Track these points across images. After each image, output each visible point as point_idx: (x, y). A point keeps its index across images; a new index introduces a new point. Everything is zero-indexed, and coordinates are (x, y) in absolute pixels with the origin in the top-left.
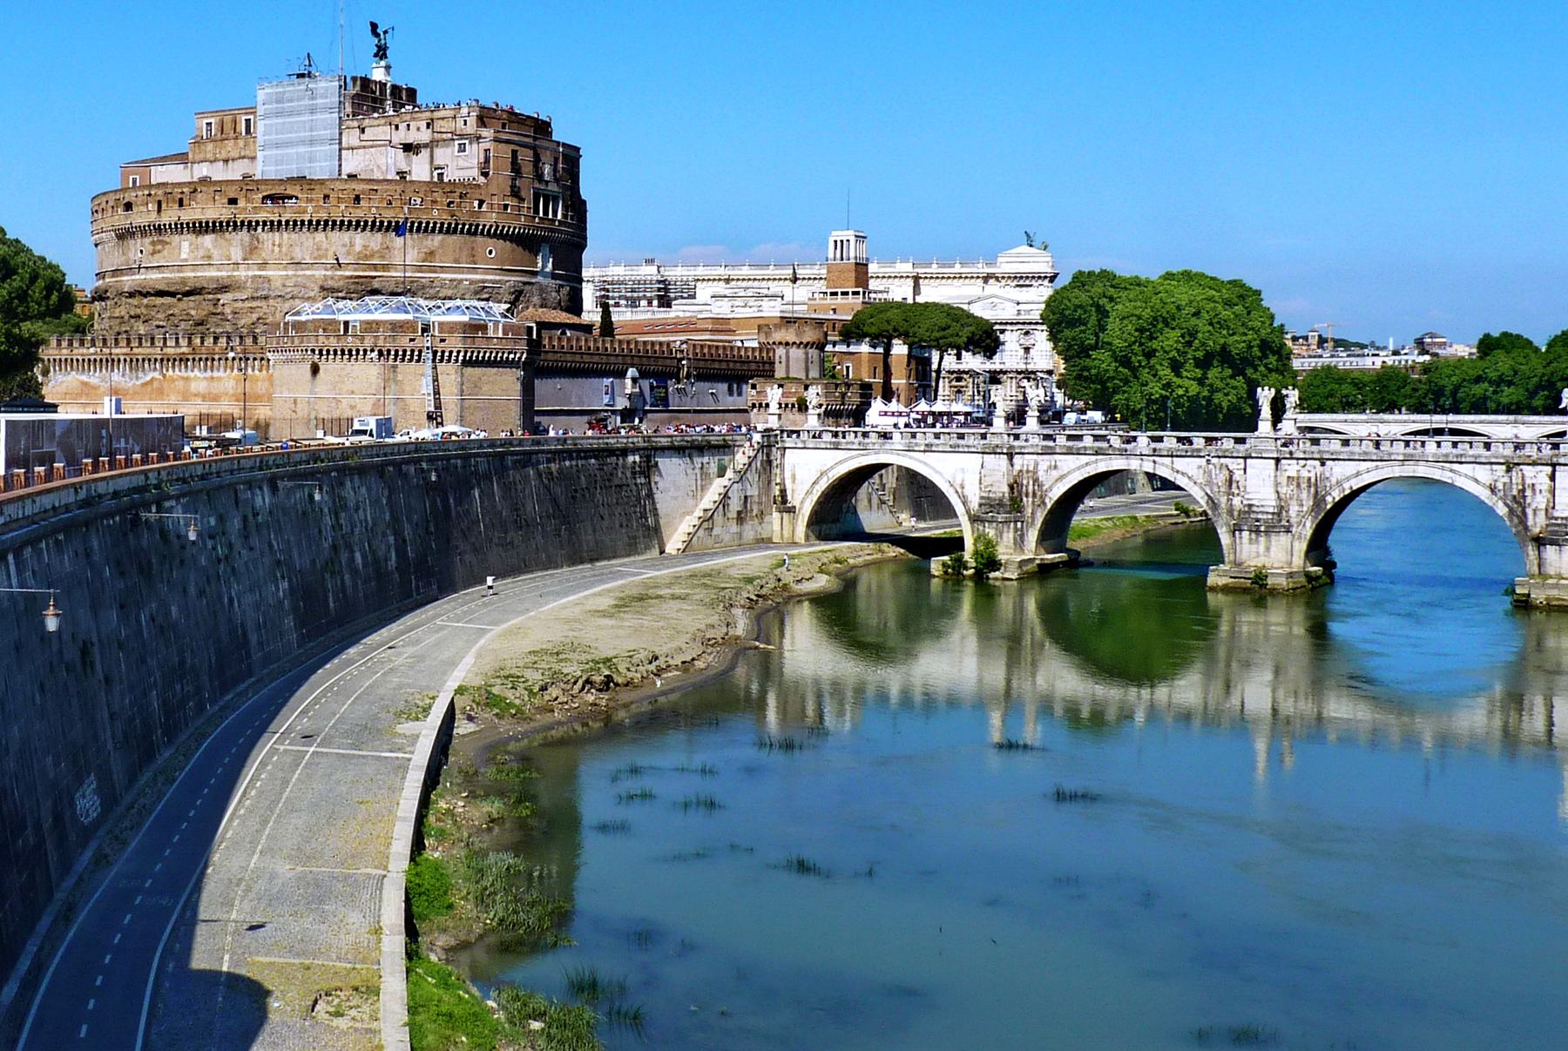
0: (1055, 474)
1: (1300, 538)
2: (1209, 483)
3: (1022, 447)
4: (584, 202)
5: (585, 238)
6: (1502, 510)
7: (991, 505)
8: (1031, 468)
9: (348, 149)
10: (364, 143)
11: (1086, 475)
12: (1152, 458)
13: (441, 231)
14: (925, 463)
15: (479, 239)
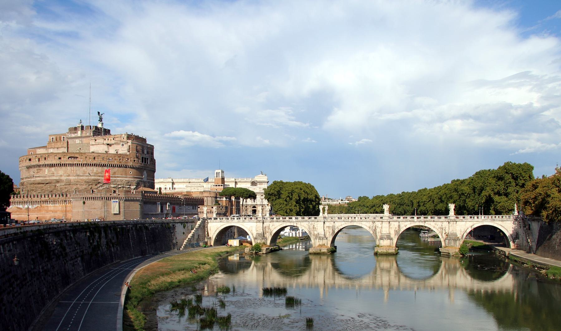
0: (274, 227)
1: (329, 240)
2: (309, 228)
3: (266, 221)
4: (155, 160)
5: (155, 169)
6: (371, 232)
7: (258, 234)
8: (268, 226)
9: (92, 145)
10: (96, 144)
11: (281, 227)
12: (296, 223)
13: (117, 167)
14: (243, 225)
15: (128, 169)
